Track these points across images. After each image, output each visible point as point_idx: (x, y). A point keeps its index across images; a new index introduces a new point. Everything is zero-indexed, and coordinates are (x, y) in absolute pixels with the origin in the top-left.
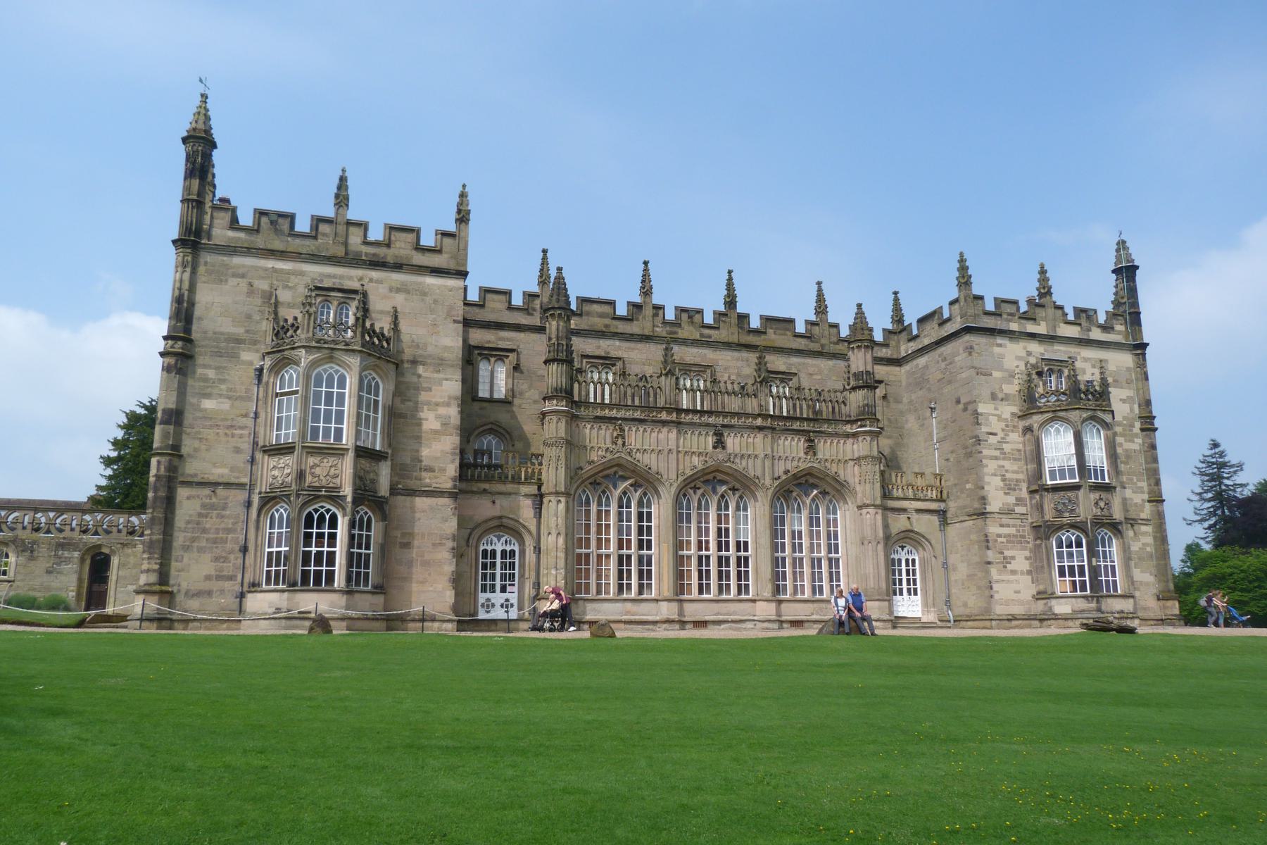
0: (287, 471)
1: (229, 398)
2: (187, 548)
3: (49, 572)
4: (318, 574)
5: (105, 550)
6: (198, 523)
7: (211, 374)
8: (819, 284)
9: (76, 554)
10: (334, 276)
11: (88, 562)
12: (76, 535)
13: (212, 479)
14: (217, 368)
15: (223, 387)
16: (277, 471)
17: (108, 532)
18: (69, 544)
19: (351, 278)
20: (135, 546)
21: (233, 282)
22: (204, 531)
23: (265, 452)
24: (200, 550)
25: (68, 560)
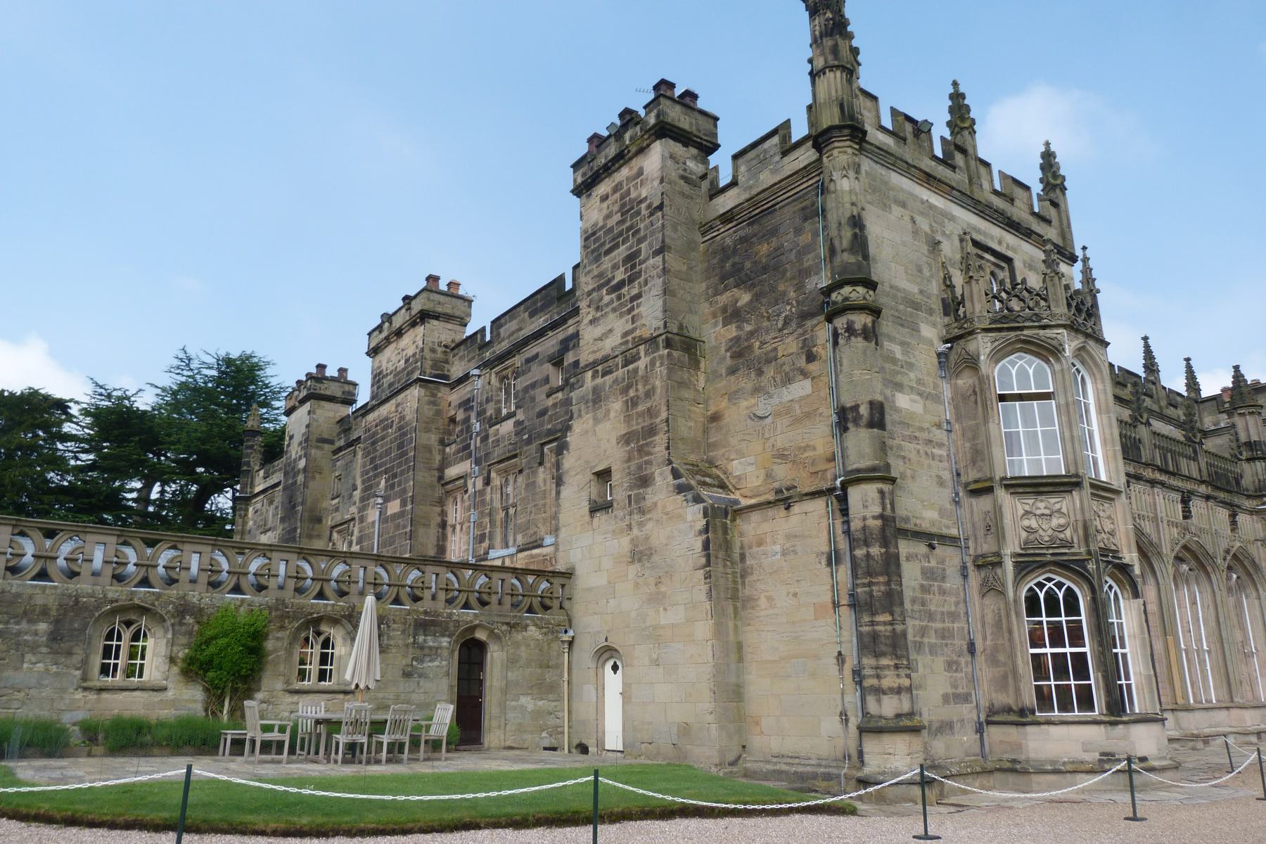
0: (1055, 522)
1: (920, 394)
2: (919, 647)
3: (407, 675)
4: (1064, 691)
5: (481, 635)
6: (923, 604)
7: (897, 351)
8: (1145, 339)
9: (445, 641)
10: (985, 234)
11: (457, 653)
12: (440, 605)
13: (925, 526)
14: (902, 344)
15: (912, 375)
16: (1021, 520)
17: (483, 604)
18: (433, 623)
19: (992, 238)
20: (525, 628)
21: (897, 211)
22: (931, 616)
23: (1007, 486)
24: (933, 650)
25: (434, 653)
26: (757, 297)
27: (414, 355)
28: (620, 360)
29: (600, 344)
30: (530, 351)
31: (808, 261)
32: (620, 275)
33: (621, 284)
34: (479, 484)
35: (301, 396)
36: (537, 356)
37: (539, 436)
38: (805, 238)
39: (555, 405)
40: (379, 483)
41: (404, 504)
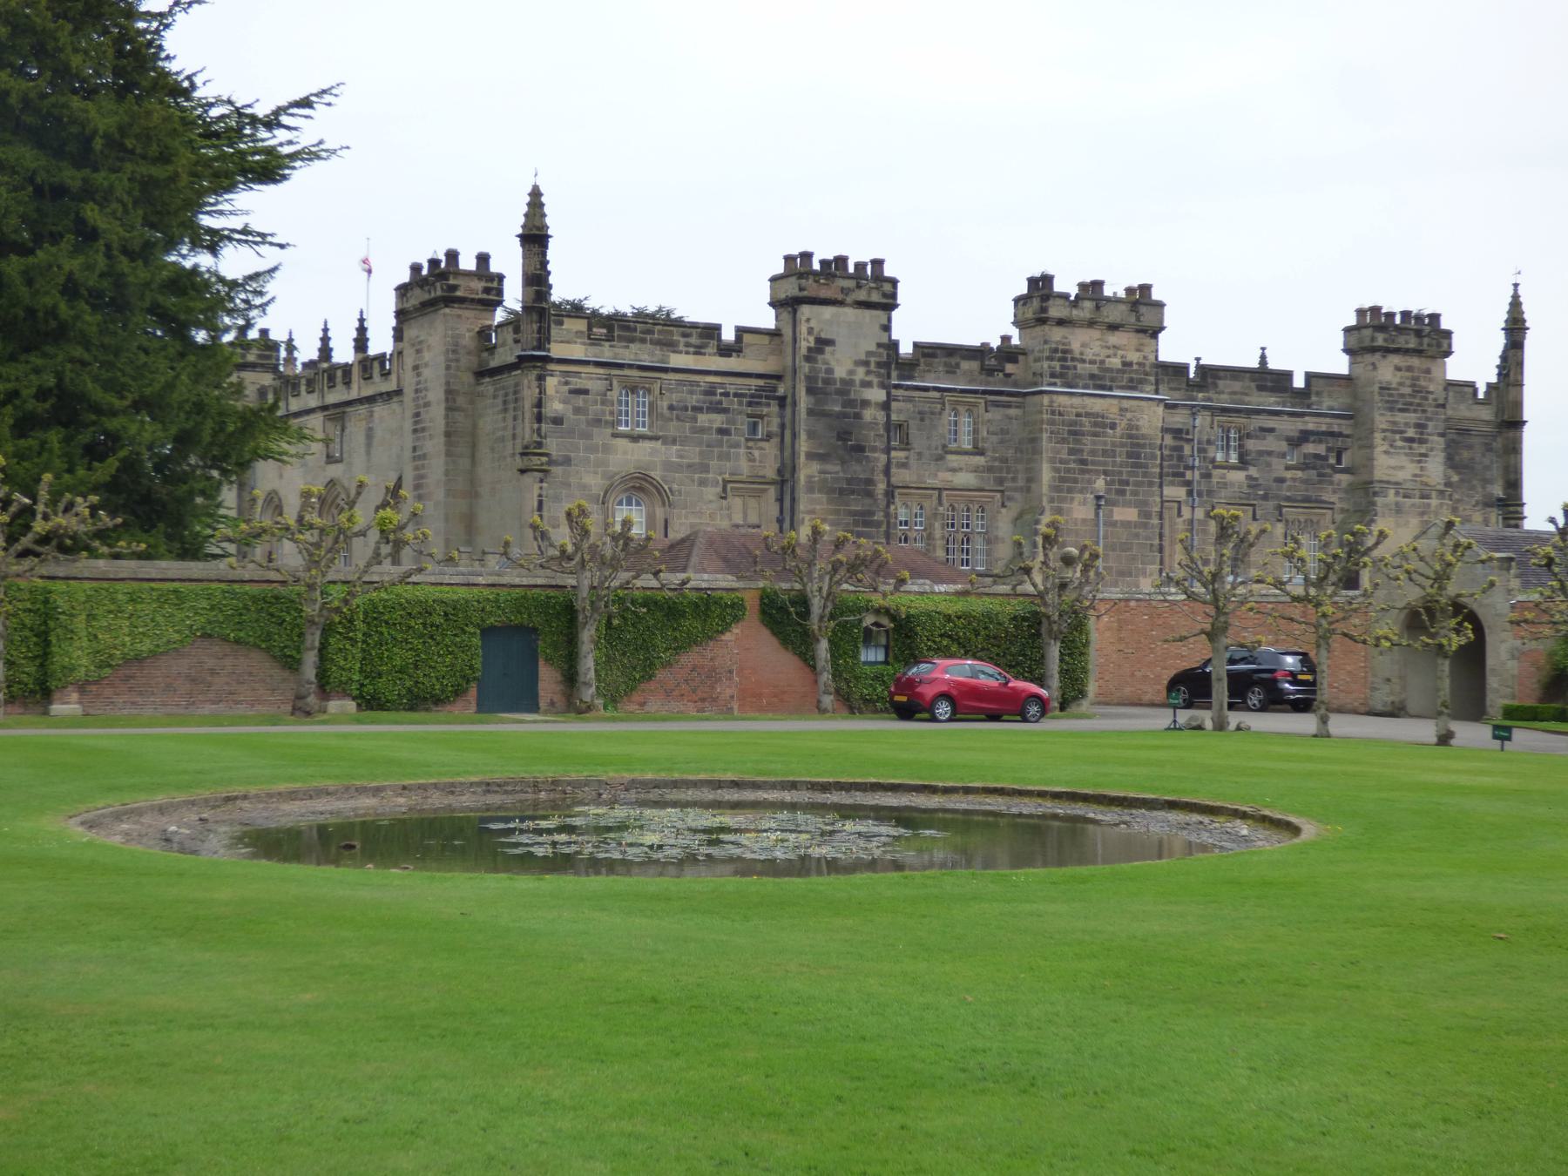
26: (1462, 480)
27: (1139, 364)
28: (1417, 493)
29: (1391, 472)
30: (1270, 422)
31: (1488, 475)
32: (1411, 433)
33: (1411, 440)
34: (1200, 514)
35: (862, 295)
36: (1271, 430)
37: (1277, 497)
38: (1486, 461)
39: (1294, 480)
40: (1090, 482)
41: (1147, 515)
